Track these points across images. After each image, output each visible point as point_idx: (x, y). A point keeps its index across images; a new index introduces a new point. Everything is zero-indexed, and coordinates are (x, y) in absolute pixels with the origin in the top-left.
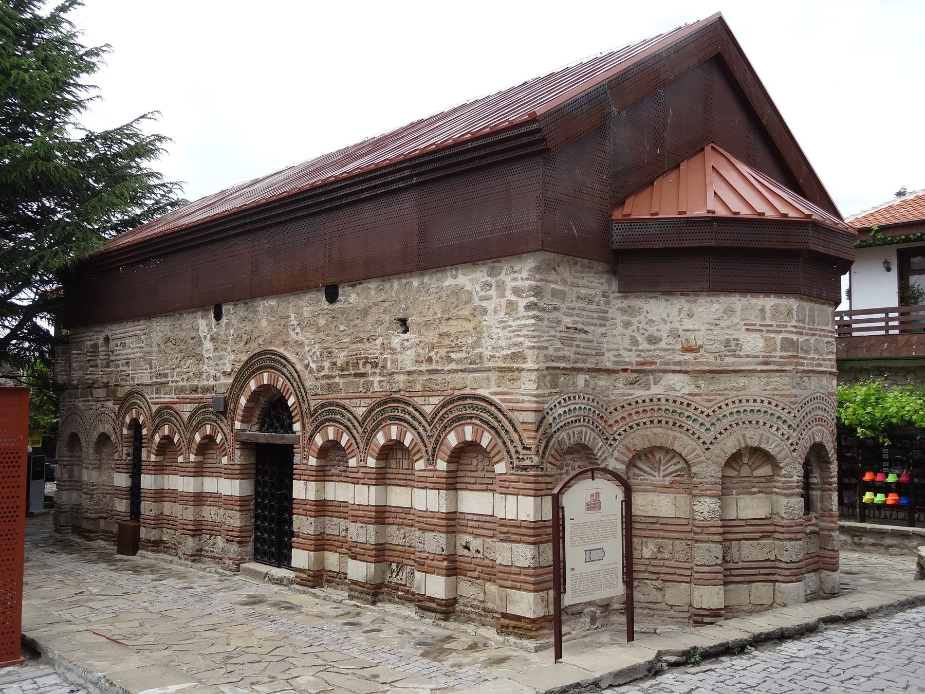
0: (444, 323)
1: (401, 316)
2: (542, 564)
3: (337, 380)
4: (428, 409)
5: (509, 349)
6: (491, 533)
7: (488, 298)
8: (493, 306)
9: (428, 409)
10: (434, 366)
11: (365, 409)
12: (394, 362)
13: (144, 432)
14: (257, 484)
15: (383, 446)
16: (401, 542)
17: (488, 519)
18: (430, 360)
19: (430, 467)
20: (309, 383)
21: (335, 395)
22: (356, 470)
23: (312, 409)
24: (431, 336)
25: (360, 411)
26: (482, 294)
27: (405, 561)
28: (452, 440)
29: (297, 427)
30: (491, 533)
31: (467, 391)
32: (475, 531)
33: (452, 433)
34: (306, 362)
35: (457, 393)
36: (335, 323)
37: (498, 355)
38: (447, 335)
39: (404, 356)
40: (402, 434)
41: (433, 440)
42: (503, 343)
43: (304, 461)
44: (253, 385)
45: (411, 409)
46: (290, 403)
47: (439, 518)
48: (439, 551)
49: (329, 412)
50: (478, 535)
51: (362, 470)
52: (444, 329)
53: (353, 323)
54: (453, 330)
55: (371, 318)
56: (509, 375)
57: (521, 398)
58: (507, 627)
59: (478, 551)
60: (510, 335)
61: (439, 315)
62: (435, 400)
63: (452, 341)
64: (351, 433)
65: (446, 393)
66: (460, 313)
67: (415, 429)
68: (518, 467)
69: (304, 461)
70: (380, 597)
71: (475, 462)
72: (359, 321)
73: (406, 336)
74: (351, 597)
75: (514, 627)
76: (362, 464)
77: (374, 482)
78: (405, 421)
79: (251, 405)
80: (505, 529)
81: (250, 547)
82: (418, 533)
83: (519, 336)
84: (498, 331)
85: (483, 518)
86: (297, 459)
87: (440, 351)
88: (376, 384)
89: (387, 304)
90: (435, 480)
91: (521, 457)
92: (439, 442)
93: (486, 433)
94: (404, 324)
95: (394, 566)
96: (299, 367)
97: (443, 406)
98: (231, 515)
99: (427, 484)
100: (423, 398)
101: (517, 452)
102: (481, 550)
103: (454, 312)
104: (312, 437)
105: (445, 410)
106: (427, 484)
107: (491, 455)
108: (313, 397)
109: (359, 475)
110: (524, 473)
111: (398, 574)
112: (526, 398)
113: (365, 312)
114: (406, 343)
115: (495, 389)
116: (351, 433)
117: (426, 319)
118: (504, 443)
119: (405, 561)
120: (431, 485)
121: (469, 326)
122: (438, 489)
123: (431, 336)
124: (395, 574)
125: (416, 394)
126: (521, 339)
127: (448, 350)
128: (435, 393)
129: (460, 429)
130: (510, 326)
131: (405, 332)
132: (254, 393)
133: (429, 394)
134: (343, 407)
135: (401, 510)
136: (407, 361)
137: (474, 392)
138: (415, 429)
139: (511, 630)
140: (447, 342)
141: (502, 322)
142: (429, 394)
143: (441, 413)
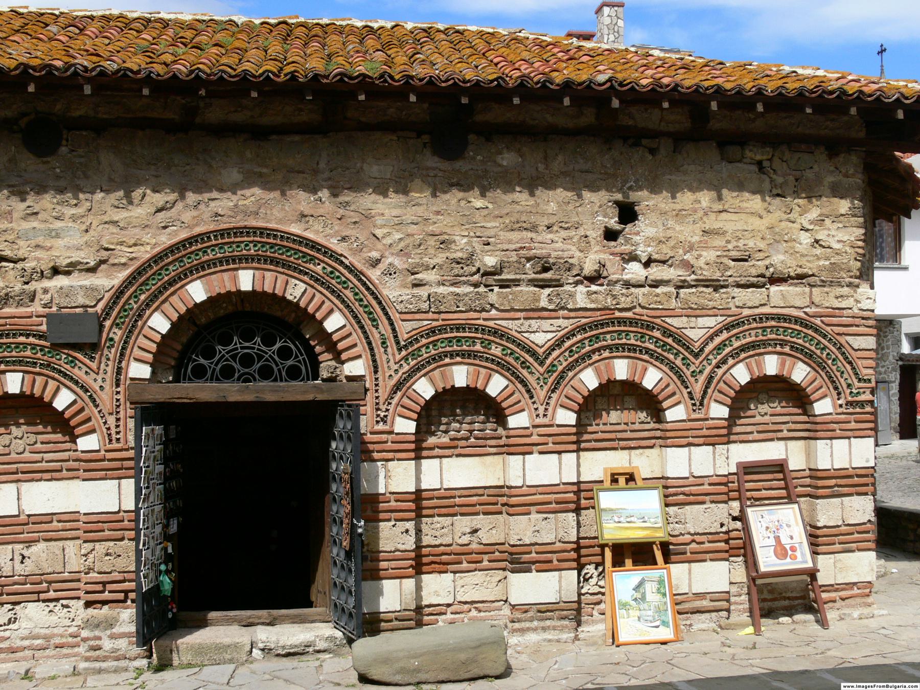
0: (713, 216)
5: (827, 259)
35: (746, 312)
41: (702, 378)
48: (715, 528)
52: (712, 223)
54: (729, 227)
62: (711, 322)
63: (728, 242)
66: (745, 205)
68: (850, 404)
87: (704, 253)
90: (705, 432)
91: (854, 391)
100: (685, 319)
120: (701, 440)
122: (713, 445)
127: (719, 253)
128: (710, 312)
129: (752, 360)
133: (698, 312)
140: (719, 242)
142: (698, 312)
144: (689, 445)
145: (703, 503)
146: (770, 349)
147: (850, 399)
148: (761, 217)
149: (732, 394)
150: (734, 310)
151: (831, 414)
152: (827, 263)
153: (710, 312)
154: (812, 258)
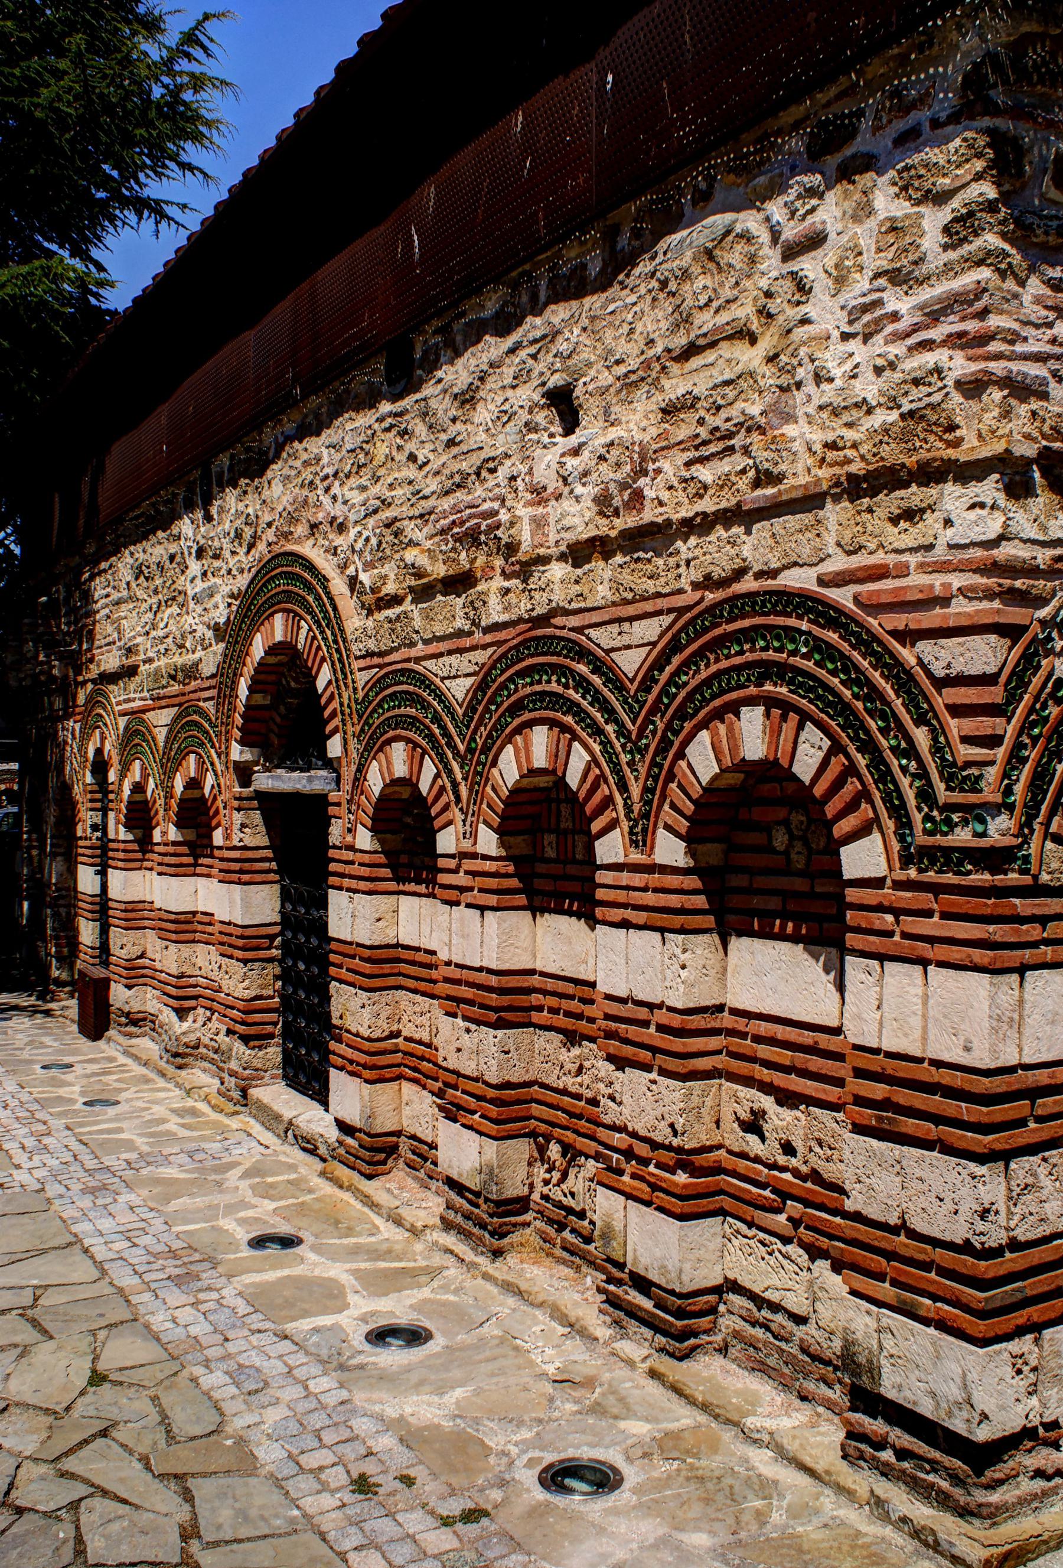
0: (675, 368)
1: (555, 380)
2: (1023, 1234)
3: (407, 605)
4: (630, 662)
5: (893, 403)
6: (831, 1093)
7: (815, 241)
8: (830, 261)
9: (630, 662)
10: (649, 515)
11: (469, 681)
12: (539, 523)
13: (112, 776)
14: (285, 896)
15: (515, 792)
16: (570, 1082)
17: (825, 1041)
18: (638, 496)
19: (636, 857)
20: (354, 621)
21: (404, 653)
22: (452, 864)
23: (360, 695)
24: (638, 421)
25: (459, 689)
26: (791, 232)
27: (582, 1143)
28: (702, 760)
29: (334, 747)
30: (831, 1093)
31: (748, 584)
32: (779, 1079)
33: (704, 736)
34: (351, 571)
36: (411, 446)
37: (850, 435)
38: (688, 403)
39: (567, 504)
40: (560, 756)
42: (868, 388)
43: (349, 838)
44: (258, 649)
45: (582, 668)
46: (321, 684)
47: (661, 1028)
48: (662, 1134)
49: (400, 700)
50: (787, 1099)
51: (468, 864)
53: (444, 437)
55: (483, 414)
56: (890, 502)
57: (937, 582)
58: (880, 1445)
59: (788, 1149)
60: (897, 350)
61: (659, 349)
62: (649, 630)
64: (442, 757)
65: (679, 601)
66: (724, 317)
67: (597, 731)
68: (929, 856)
69: (349, 838)
70: (515, 1238)
71: (780, 840)
72: (459, 426)
73: (573, 440)
74: (447, 1225)
75: (902, 1454)
76: (466, 845)
77: (492, 900)
78: (572, 708)
79: (259, 699)
80: (879, 1091)
81: (274, 1052)
82: (606, 1068)
83: (927, 345)
84: (853, 345)
85: (807, 1037)
86: (336, 832)
88: (493, 600)
89: (523, 354)
90: (650, 898)
92: (662, 776)
93: (811, 732)
94: (564, 405)
95: (554, 1151)
96: (338, 585)
97: (675, 646)
98: (231, 970)
99: (629, 914)
100: (614, 628)
101: (926, 796)
102: (798, 1144)
103: (706, 321)
104: (361, 769)
105: (676, 660)
106: (629, 914)
107: (831, 809)
108: (362, 663)
109: (461, 879)
110: (950, 878)
111: (564, 1176)
112: (957, 581)
113: (467, 399)
114: (571, 462)
115: (838, 563)
116: (442, 757)
117: (621, 370)
118: (877, 761)
119: (582, 1143)
120: (640, 917)
121: (750, 357)
122: (662, 930)
123: (638, 421)
124: (556, 1175)
125: (595, 617)
126: (930, 359)
130: (895, 316)
131: (568, 431)
132: (262, 667)
134: (423, 681)
135: (570, 989)
136: (577, 517)
137: (770, 584)
138: (597, 731)
139: (887, 1455)
141: (865, 309)
142: (630, 610)
143: (664, 677)
144: (625, 924)
145: (647, 1068)
146: (752, 690)
147: (921, 839)
148: (753, 340)
149: (689, 807)
150: (691, 597)
151: (878, 883)
152: (894, 416)
153: (648, 607)
154: (855, 414)
